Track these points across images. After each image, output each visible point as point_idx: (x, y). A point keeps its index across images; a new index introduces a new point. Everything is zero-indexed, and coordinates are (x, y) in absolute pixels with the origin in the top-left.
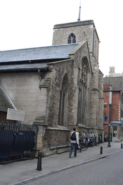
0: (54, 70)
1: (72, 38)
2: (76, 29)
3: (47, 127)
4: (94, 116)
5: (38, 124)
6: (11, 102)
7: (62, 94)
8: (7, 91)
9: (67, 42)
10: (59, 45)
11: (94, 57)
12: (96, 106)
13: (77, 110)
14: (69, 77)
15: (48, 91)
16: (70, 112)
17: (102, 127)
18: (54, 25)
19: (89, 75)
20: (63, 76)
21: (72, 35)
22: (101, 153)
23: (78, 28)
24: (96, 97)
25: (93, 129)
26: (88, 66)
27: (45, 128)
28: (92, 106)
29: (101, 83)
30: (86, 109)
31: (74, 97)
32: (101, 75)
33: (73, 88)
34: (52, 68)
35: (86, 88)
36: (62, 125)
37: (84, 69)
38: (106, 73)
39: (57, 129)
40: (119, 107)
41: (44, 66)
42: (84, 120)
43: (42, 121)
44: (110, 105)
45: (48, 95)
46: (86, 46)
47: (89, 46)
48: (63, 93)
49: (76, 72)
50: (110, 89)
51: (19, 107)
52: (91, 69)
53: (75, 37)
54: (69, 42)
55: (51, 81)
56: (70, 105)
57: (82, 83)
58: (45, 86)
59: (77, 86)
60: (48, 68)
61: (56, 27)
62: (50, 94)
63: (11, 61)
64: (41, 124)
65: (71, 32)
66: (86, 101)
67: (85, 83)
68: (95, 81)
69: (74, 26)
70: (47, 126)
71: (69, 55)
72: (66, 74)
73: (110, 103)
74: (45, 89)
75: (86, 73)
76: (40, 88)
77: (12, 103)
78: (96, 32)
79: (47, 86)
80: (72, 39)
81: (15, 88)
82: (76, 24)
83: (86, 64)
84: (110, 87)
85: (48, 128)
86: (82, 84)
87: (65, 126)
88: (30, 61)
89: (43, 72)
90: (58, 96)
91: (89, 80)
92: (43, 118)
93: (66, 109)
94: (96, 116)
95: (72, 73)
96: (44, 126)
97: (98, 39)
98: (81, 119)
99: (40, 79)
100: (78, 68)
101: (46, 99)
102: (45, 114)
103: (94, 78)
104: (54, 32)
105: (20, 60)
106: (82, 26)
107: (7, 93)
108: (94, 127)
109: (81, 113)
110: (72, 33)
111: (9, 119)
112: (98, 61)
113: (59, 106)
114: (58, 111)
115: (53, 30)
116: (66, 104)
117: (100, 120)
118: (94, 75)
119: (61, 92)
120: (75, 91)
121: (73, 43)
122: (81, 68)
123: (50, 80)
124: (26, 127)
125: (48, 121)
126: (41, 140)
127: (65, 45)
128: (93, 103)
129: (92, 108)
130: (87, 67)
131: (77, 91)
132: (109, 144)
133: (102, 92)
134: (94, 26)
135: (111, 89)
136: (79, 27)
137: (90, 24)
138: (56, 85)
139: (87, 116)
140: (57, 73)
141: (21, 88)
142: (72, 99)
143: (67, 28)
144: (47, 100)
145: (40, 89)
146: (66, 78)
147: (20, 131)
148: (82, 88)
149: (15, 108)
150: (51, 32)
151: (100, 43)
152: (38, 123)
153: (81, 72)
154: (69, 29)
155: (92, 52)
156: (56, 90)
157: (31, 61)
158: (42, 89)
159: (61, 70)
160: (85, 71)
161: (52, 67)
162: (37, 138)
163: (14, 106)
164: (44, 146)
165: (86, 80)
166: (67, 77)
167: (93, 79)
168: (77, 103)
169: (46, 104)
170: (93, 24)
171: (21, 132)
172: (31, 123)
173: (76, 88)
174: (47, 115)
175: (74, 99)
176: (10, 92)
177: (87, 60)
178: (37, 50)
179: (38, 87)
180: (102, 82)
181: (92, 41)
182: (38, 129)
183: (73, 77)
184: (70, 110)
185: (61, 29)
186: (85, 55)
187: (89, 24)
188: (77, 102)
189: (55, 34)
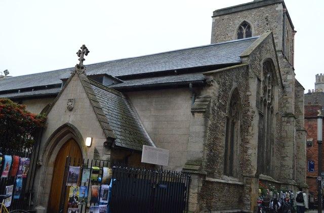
0: (216, 83)
1: (245, 30)
3: (205, 178)
4: (289, 162)
5: (191, 171)
7: (230, 123)
9: (237, 36)
10: (223, 42)
11: (286, 58)
12: (291, 143)
13: (257, 150)
14: (242, 95)
15: (206, 117)
16: (245, 154)
17: (304, 182)
18: (214, 10)
19: (277, 91)
20: (230, 93)
21: (245, 24)
23: (254, 12)
24: (291, 128)
25: (286, 184)
26: (274, 75)
27: (202, 179)
28: (284, 143)
30: (273, 148)
31: (250, 128)
34: (212, 81)
35: (272, 112)
36: (231, 174)
37: (267, 80)
39: (223, 181)
41: (199, 77)
42: (269, 167)
43: (197, 168)
44: (319, 143)
45: (205, 125)
46: (270, 40)
47: (275, 41)
48: (230, 121)
49: (253, 85)
50: (318, 113)
51: (159, 143)
52: (281, 80)
53: (249, 27)
54: (240, 36)
55: (210, 101)
56: (245, 141)
58: (201, 110)
59: (255, 109)
60: (205, 80)
61: (216, 14)
62: (210, 122)
63: (147, 72)
64: (196, 172)
66: (272, 134)
67: (270, 104)
68: (289, 100)
69: (248, 9)
70: (204, 176)
72: (236, 89)
73: (320, 138)
74: (202, 114)
75: (272, 86)
76: (193, 113)
77: (148, 137)
79: (204, 110)
80: (244, 31)
82: (251, 6)
83: (271, 71)
84: (319, 111)
85: (207, 179)
86: (265, 105)
89: (197, 89)
90: (222, 126)
92: (198, 161)
93: (237, 148)
94: (292, 162)
95: (247, 88)
96: (201, 175)
97: (293, 28)
98: (264, 165)
99: (193, 98)
100: (256, 79)
101: (203, 131)
102: (201, 155)
103: (286, 95)
104: (213, 23)
105: (160, 70)
106: (262, 8)
107: (141, 122)
108: (289, 181)
109: (265, 155)
110: (245, 22)
111: (144, 162)
112: (293, 65)
113: (224, 143)
114: (223, 151)
115: (212, 19)
116: (238, 141)
117: (300, 170)
118: (287, 90)
119: (228, 120)
121: (247, 37)
122: (262, 79)
123: (209, 99)
124: (171, 176)
125: (207, 167)
126: (196, 199)
127: (233, 41)
128: (286, 139)
129: (284, 147)
130: (273, 77)
133: (302, 118)
134: (284, 6)
136: (256, 10)
137: (277, 3)
138: (218, 107)
139: (275, 161)
140: (220, 87)
142: (247, 132)
144: (205, 132)
145: (193, 114)
146: (236, 95)
147: (161, 182)
148: (266, 112)
149: (153, 144)
150: (210, 21)
151: (296, 33)
152: (192, 170)
153: (262, 85)
154: (239, 15)
155: (281, 51)
156: (219, 117)
157: (177, 70)
158: (196, 114)
160: (269, 83)
161: (211, 78)
162: (188, 195)
163: (151, 142)
164: (201, 209)
165: (272, 99)
166: (238, 93)
167: (285, 97)
169: (203, 139)
171: (164, 183)
172: (179, 170)
173: (254, 112)
174: (205, 157)
176: (145, 120)
177: (273, 65)
178: (186, 53)
180: (302, 101)
181: (282, 32)
182: (190, 180)
183: (248, 93)
184: (245, 150)
185: (226, 17)
186: (268, 56)
187: (274, 4)
189: (215, 26)
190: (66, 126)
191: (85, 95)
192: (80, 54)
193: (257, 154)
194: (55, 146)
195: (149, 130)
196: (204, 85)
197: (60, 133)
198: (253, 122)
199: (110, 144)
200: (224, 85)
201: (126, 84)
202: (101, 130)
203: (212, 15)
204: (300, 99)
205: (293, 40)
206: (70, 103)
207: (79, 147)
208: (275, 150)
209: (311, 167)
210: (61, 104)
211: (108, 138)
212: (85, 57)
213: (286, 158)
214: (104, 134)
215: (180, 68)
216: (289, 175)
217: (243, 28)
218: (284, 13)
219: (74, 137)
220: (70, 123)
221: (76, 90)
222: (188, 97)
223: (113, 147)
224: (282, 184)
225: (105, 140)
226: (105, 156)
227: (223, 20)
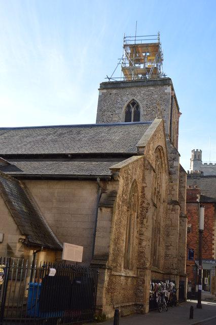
2: (139, 92)
4: (173, 251)
6: (49, 227)
8: (42, 209)
21: (134, 103)
22: (191, 317)
23: (144, 90)
29: (182, 189)
31: (145, 220)
32: (183, 173)
33: (144, 205)
44: (201, 232)
49: (150, 177)
50: (197, 198)
53: (138, 107)
57: (157, 193)
59: (150, 202)
60: (112, 176)
62: (116, 218)
65: (131, 98)
68: (175, 187)
71: (138, 147)
73: (202, 227)
78: (175, 98)
80: (133, 110)
81: (55, 205)
84: (198, 195)
87: (131, 270)
88: (69, 156)
95: (144, 179)
97: (178, 109)
103: (172, 182)
104: (99, 96)
107: (41, 214)
108: (172, 271)
110: (133, 99)
120: (147, 210)
129: (168, 235)
130: (162, 164)
131: (151, 209)
132: (199, 302)
134: (173, 89)
135: (199, 198)
137: (166, 85)
138: (123, 202)
139: (161, 250)
140: (124, 182)
141: (67, 206)
143: (124, 90)
145: (101, 209)
154: (128, 91)
157: (73, 155)
158: (104, 209)
159: (130, 177)
163: (53, 235)
168: (151, 230)
173: (148, 204)
176: (46, 212)
180: (185, 187)
181: (170, 116)
185: (114, 91)
188: (150, 229)
189: (102, 100)
193: (150, 245)
195: (50, 222)
196: (112, 179)
200: (127, 178)
203: (99, 88)
204: (183, 185)
205: (178, 122)
208: (161, 239)
209: (191, 255)
213: (170, 247)
214: (18, 230)
216: (172, 265)
217: (131, 106)
218: (172, 96)
222: (95, 190)
223: (26, 243)
224: (166, 274)
227: (111, 94)
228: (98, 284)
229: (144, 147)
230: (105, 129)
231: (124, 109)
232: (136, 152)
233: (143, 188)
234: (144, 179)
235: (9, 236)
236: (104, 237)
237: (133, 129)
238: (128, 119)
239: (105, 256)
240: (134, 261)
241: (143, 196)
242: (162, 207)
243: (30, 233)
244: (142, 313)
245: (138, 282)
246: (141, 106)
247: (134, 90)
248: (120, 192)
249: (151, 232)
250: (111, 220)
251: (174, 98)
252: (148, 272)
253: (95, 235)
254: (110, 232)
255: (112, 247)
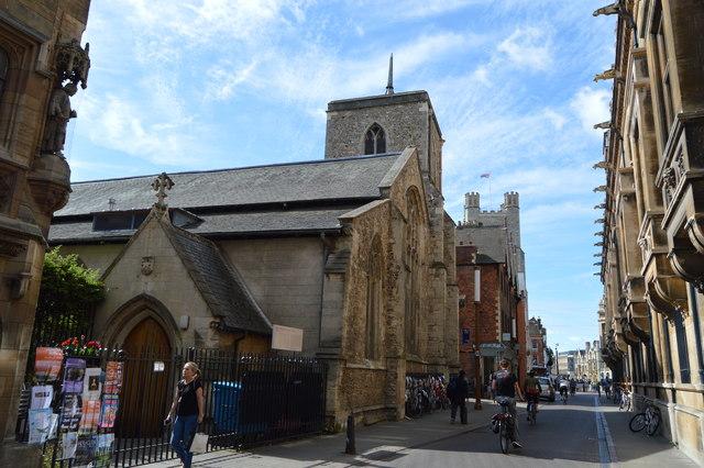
4: (438, 333)
5: (327, 357)
8: (246, 280)
17: (456, 357)
21: (376, 128)
23: (389, 110)
24: (441, 284)
29: (449, 246)
31: (394, 290)
33: (392, 269)
36: (372, 357)
38: (459, 215)
40: (498, 305)
41: (328, 220)
44: (476, 303)
45: (343, 291)
48: (371, 282)
53: (382, 133)
56: (389, 309)
57: (411, 252)
59: (400, 264)
66: (417, 295)
73: (478, 298)
78: (435, 119)
86: (409, 252)
91: (422, 242)
93: (380, 321)
95: (390, 233)
97: (440, 135)
98: (410, 336)
110: (375, 124)
117: (452, 342)
129: (431, 311)
131: (403, 274)
132: (478, 401)
134: (430, 107)
139: (422, 332)
141: (280, 275)
146: (377, 246)
150: (322, 116)
157: (288, 203)
158: (332, 277)
163: (264, 316)
170: (428, 101)
175: (394, 294)
179: (319, 271)
182: (327, 369)
185: (348, 114)
190: (142, 297)
191: (172, 252)
192: (157, 186)
194: (121, 330)
196: (341, 234)
197: (128, 312)
198: (397, 281)
199: (220, 328)
201: (211, 225)
202: (203, 306)
204: (450, 240)
205: (440, 153)
206: (146, 264)
207: (164, 332)
208: (421, 316)
209: (465, 337)
210: (131, 261)
211: (215, 317)
212: (166, 191)
215: (289, 199)
219: (155, 316)
220: (149, 294)
221: (154, 240)
225: (212, 319)
226: (211, 342)
228: (329, 382)
229: (389, 188)
230: (336, 166)
231: (363, 137)
232: (378, 194)
233: (390, 245)
234: (390, 233)
235: (197, 319)
236: (332, 316)
237: (376, 163)
238: (369, 150)
239: (338, 340)
240: (381, 348)
241: (391, 256)
242: (420, 272)
243: (226, 313)
244: (394, 419)
245: (387, 377)
246: (387, 132)
247: (376, 111)
248: (354, 250)
249: (403, 307)
250: (343, 291)
251: (433, 117)
252: (401, 362)
253: (321, 313)
254: (342, 307)
255: (346, 329)
